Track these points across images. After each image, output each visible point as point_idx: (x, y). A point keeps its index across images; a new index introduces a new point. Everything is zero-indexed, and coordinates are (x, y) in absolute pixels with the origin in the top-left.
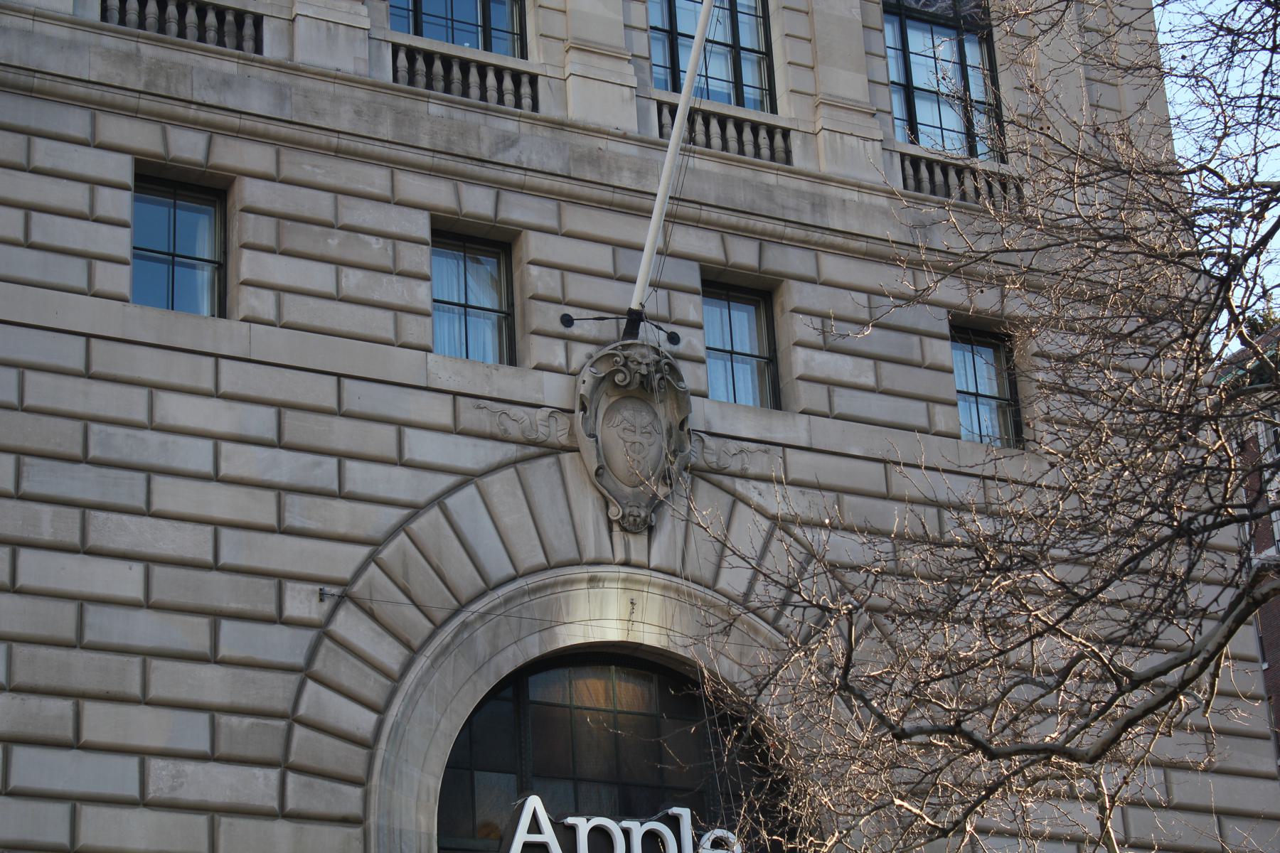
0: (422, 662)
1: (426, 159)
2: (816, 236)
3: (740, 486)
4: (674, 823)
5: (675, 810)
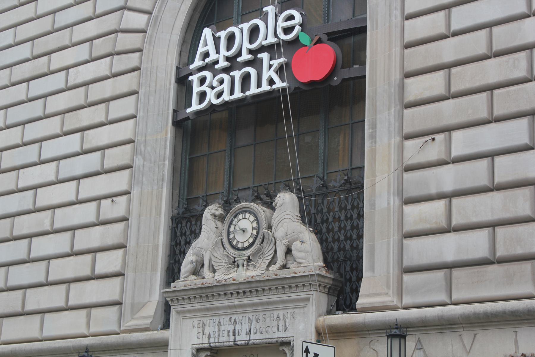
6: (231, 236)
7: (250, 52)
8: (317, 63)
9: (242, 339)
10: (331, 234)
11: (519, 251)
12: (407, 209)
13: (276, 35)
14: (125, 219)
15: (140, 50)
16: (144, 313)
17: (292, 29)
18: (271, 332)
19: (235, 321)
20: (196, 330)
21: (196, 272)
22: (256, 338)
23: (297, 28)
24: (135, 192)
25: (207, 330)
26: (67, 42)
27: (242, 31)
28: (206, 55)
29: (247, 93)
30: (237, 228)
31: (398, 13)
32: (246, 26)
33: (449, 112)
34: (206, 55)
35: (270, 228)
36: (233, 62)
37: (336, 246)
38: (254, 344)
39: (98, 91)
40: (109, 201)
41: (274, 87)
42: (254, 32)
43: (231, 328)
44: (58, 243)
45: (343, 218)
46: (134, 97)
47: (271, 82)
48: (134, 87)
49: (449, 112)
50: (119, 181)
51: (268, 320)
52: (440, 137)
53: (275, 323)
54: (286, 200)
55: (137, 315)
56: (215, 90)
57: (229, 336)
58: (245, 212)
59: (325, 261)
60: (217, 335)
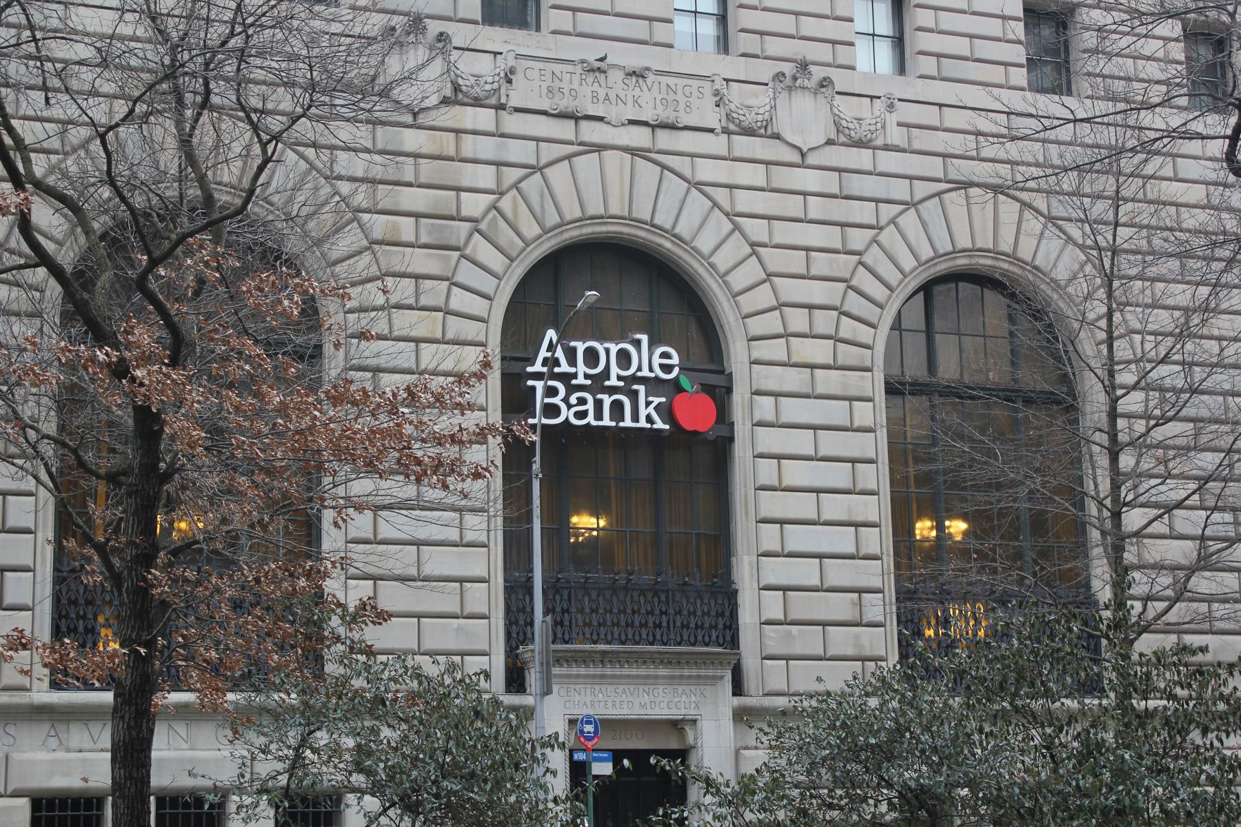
4: (637, 344)
5: (638, 336)
13: (651, 370)
23: (676, 370)
29: (621, 424)
32: (614, 348)
36: (598, 383)
47: (649, 419)
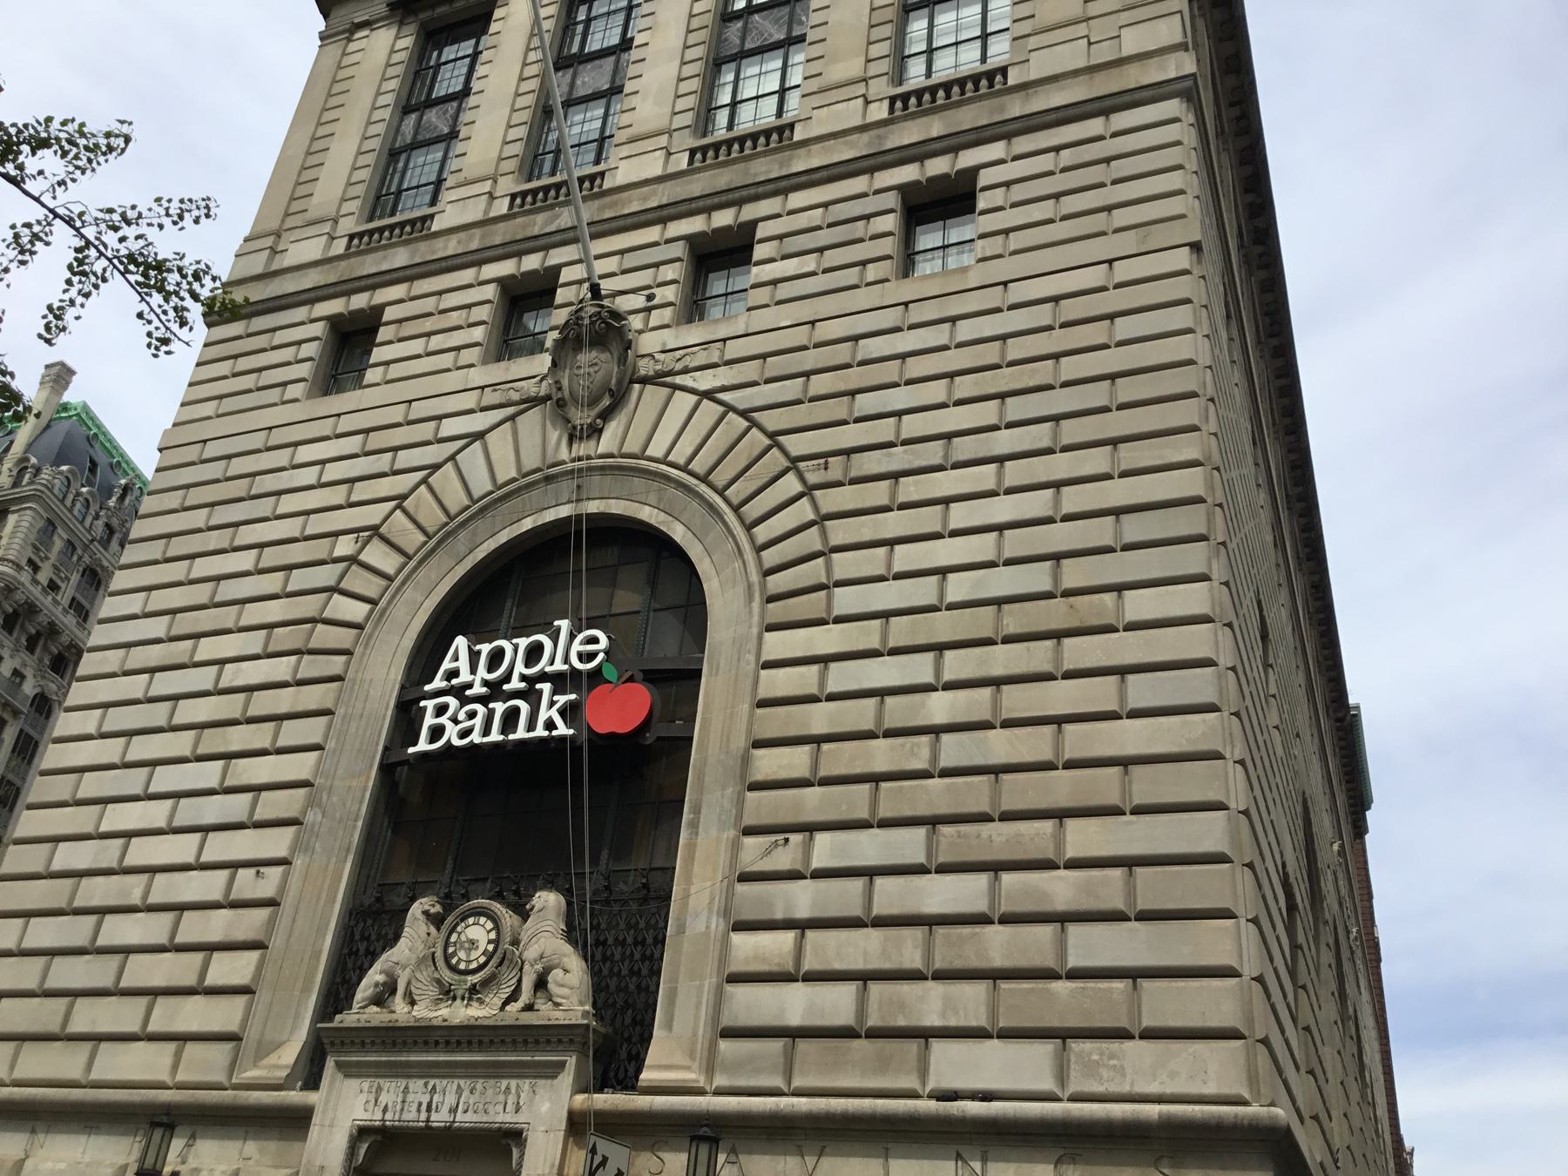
0: (412, 563)
1: (500, 251)
2: (784, 183)
3: (678, 380)
6: (451, 950)
7: (523, 678)
8: (622, 710)
9: (440, 1118)
10: (608, 964)
11: (901, 1022)
12: (738, 938)
13: (566, 660)
14: (272, 903)
15: (347, 652)
16: (272, 1059)
17: (591, 656)
18: (492, 1113)
19: (434, 1087)
20: (363, 1097)
21: (382, 997)
22: (465, 1119)
23: (601, 656)
24: (298, 862)
25: (383, 1099)
26: (230, 624)
27: (516, 647)
28: (454, 673)
29: (511, 737)
30: (463, 938)
31: (751, 658)
32: (523, 642)
33: (813, 803)
34: (454, 673)
35: (515, 942)
36: (495, 690)
37: (613, 983)
38: (460, 1129)
39: (264, 703)
40: (253, 871)
41: (555, 733)
42: (534, 653)
43: (425, 1099)
44: (151, 929)
45: (630, 940)
46: (323, 720)
47: (550, 725)
48: (329, 705)
49: (813, 803)
50: (276, 843)
51: (490, 1092)
52: (796, 838)
53: (501, 1098)
54: (548, 901)
55: (266, 1062)
56: (454, 726)
57: (419, 1111)
58: (480, 914)
59: (594, 1005)
60: (398, 1108)
